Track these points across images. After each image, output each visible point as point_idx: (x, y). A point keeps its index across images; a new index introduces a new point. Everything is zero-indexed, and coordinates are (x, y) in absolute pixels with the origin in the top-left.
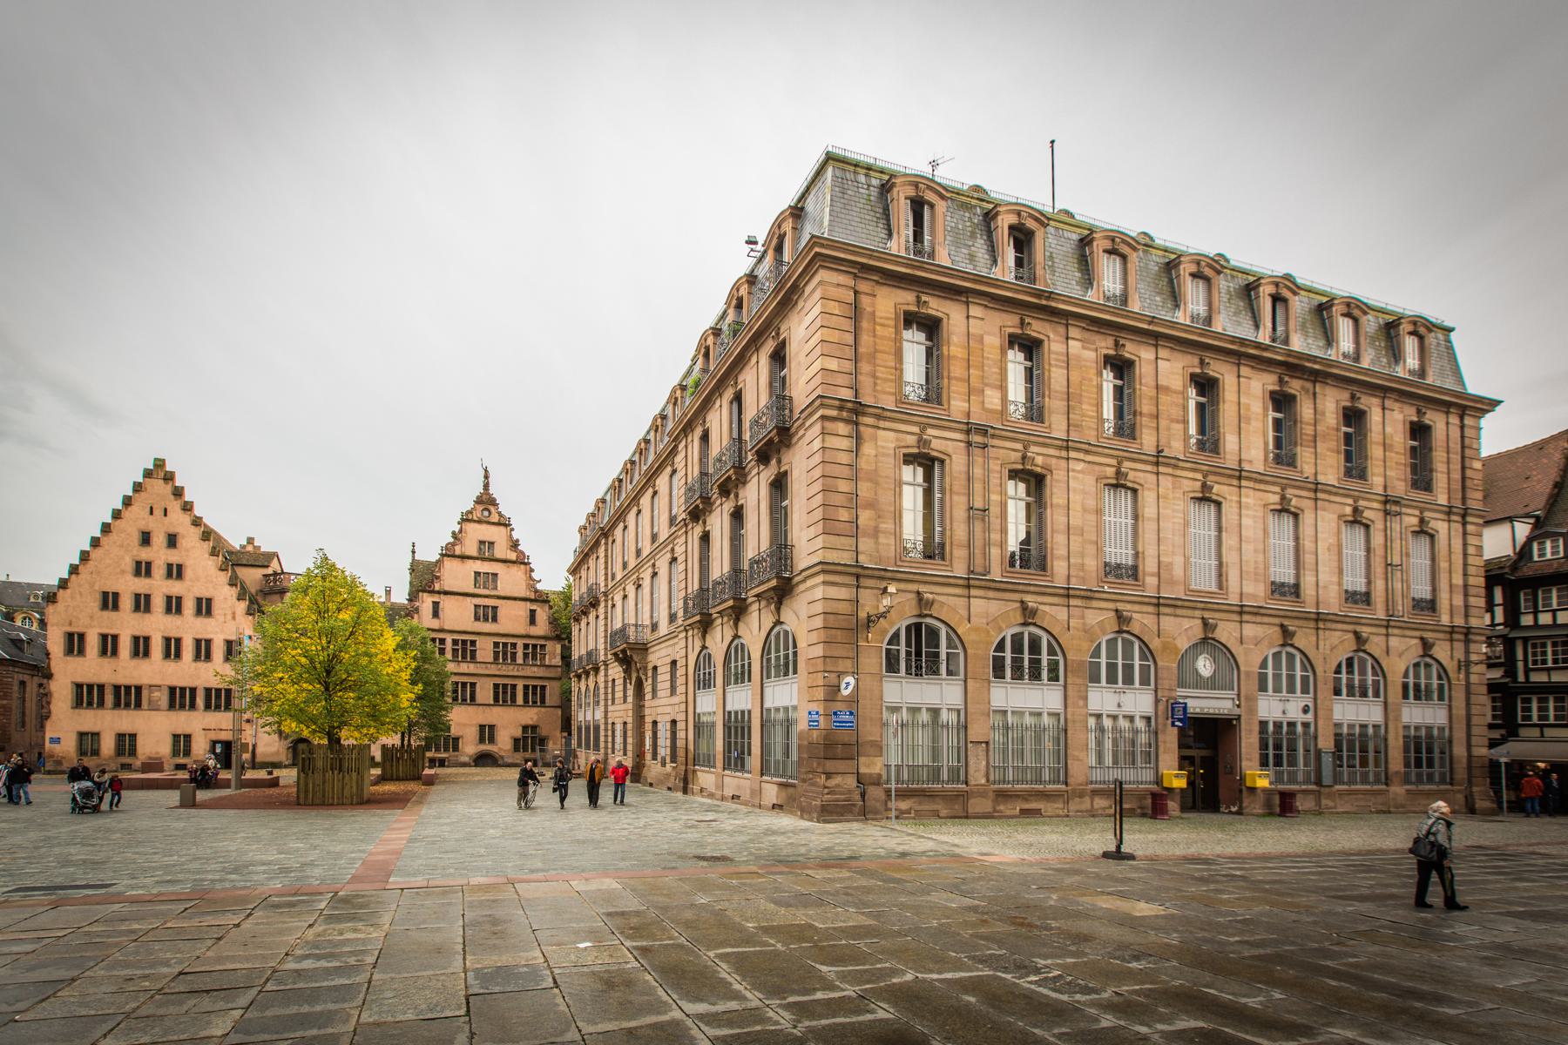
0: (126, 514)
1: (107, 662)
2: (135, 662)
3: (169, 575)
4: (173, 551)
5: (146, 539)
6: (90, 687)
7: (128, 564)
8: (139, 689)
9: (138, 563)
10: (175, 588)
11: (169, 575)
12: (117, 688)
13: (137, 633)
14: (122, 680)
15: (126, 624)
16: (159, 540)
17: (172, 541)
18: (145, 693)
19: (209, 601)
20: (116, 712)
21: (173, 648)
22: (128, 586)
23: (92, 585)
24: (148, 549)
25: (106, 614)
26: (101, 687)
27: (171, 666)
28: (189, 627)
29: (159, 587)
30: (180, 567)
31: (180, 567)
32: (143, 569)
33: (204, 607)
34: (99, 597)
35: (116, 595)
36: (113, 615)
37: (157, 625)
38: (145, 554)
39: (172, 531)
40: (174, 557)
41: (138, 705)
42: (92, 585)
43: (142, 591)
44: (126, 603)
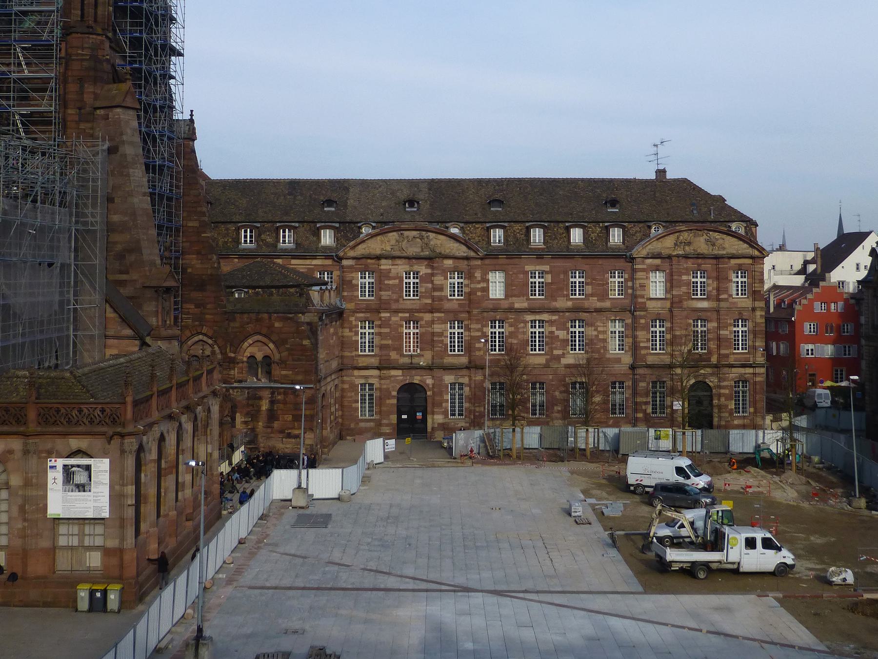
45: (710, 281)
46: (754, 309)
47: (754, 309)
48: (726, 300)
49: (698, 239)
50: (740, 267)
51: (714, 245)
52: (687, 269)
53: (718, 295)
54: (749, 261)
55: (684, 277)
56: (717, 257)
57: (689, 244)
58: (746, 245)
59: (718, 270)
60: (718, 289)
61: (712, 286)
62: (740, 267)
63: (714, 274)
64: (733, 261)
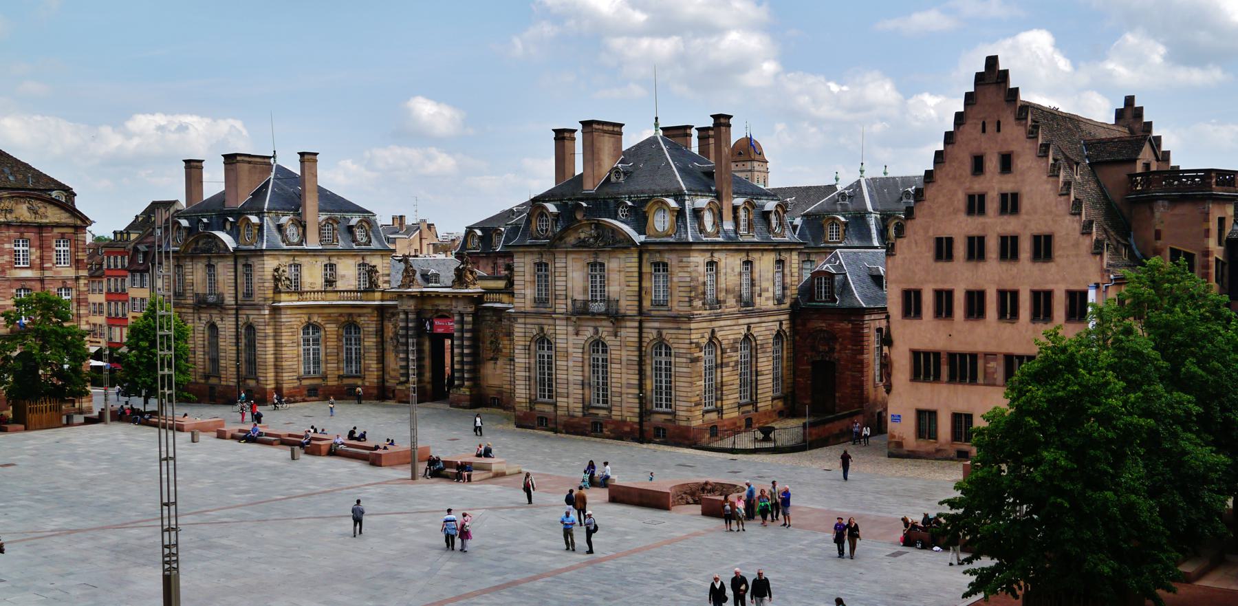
0: (959, 137)
1: (942, 324)
2: (969, 325)
3: (1003, 210)
4: (1008, 177)
5: (978, 165)
6: (927, 354)
7: (960, 200)
8: (974, 357)
9: (971, 198)
10: (1010, 225)
11: (1003, 210)
12: (952, 356)
13: (972, 287)
14: (957, 347)
15: (961, 277)
16: (992, 164)
17: (1006, 163)
18: (980, 363)
19: (1049, 239)
20: (952, 386)
21: (1008, 304)
22: (961, 227)
23: (926, 231)
24: (981, 178)
25: (940, 264)
26: (937, 355)
27: (1007, 329)
28: (1026, 276)
29: (994, 225)
30: (1015, 196)
31: (1015, 196)
32: (976, 205)
33: (1043, 248)
34: (932, 244)
35: (950, 241)
36: (946, 266)
37: (991, 275)
38: (978, 186)
39: (1005, 149)
40: (1008, 184)
41: (974, 380)
42: (926, 230)
43: (975, 233)
44: (960, 249)
45: (33, 250)
46: (77, 278)
47: (77, 278)
48: (49, 269)
49: (20, 206)
50: (63, 236)
51: (36, 213)
52: (9, 237)
53: (42, 263)
54: (71, 230)
55: (7, 246)
56: (41, 227)
57: (11, 211)
58: (67, 215)
59: (41, 239)
60: (42, 258)
61: (35, 254)
62: (63, 236)
63: (38, 243)
64: (56, 231)
